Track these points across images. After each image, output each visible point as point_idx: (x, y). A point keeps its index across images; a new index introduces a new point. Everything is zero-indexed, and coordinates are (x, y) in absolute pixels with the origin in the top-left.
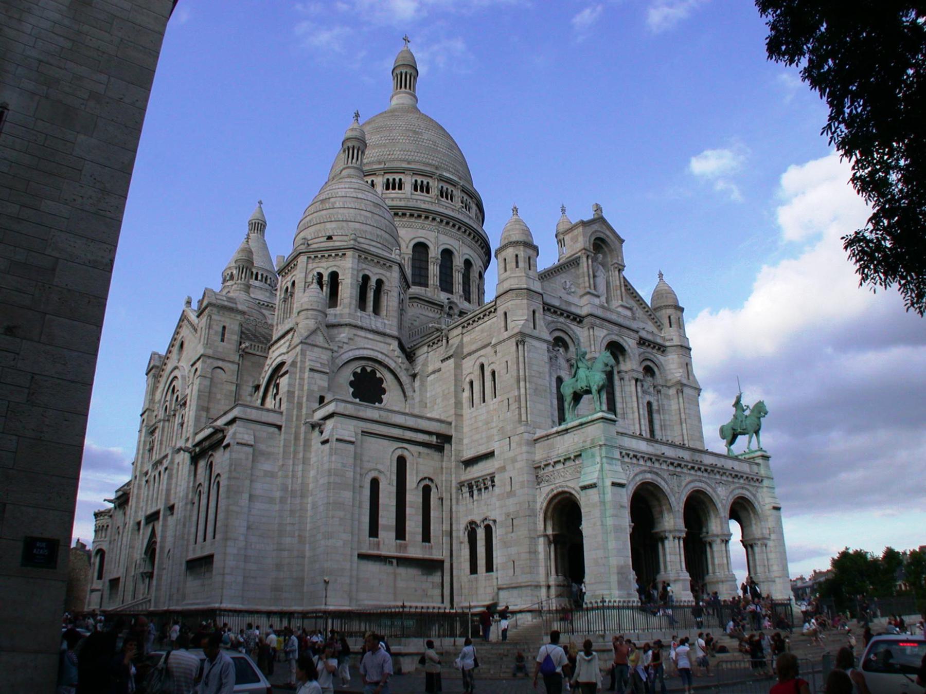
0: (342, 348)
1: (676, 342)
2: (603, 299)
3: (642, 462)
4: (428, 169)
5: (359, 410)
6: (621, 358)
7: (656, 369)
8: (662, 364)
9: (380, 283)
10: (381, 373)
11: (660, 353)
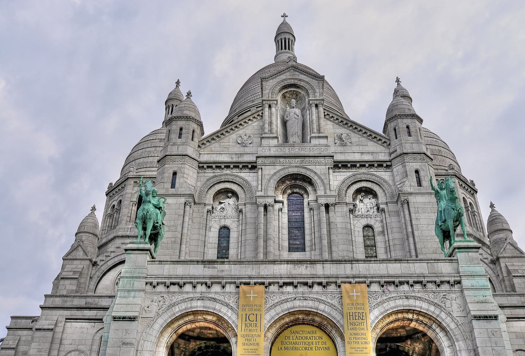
0: (109, 256)
1: (399, 152)
2: (295, 139)
5: (66, 302)
6: (309, 189)
8: (385, 181)
11: (381, 169)
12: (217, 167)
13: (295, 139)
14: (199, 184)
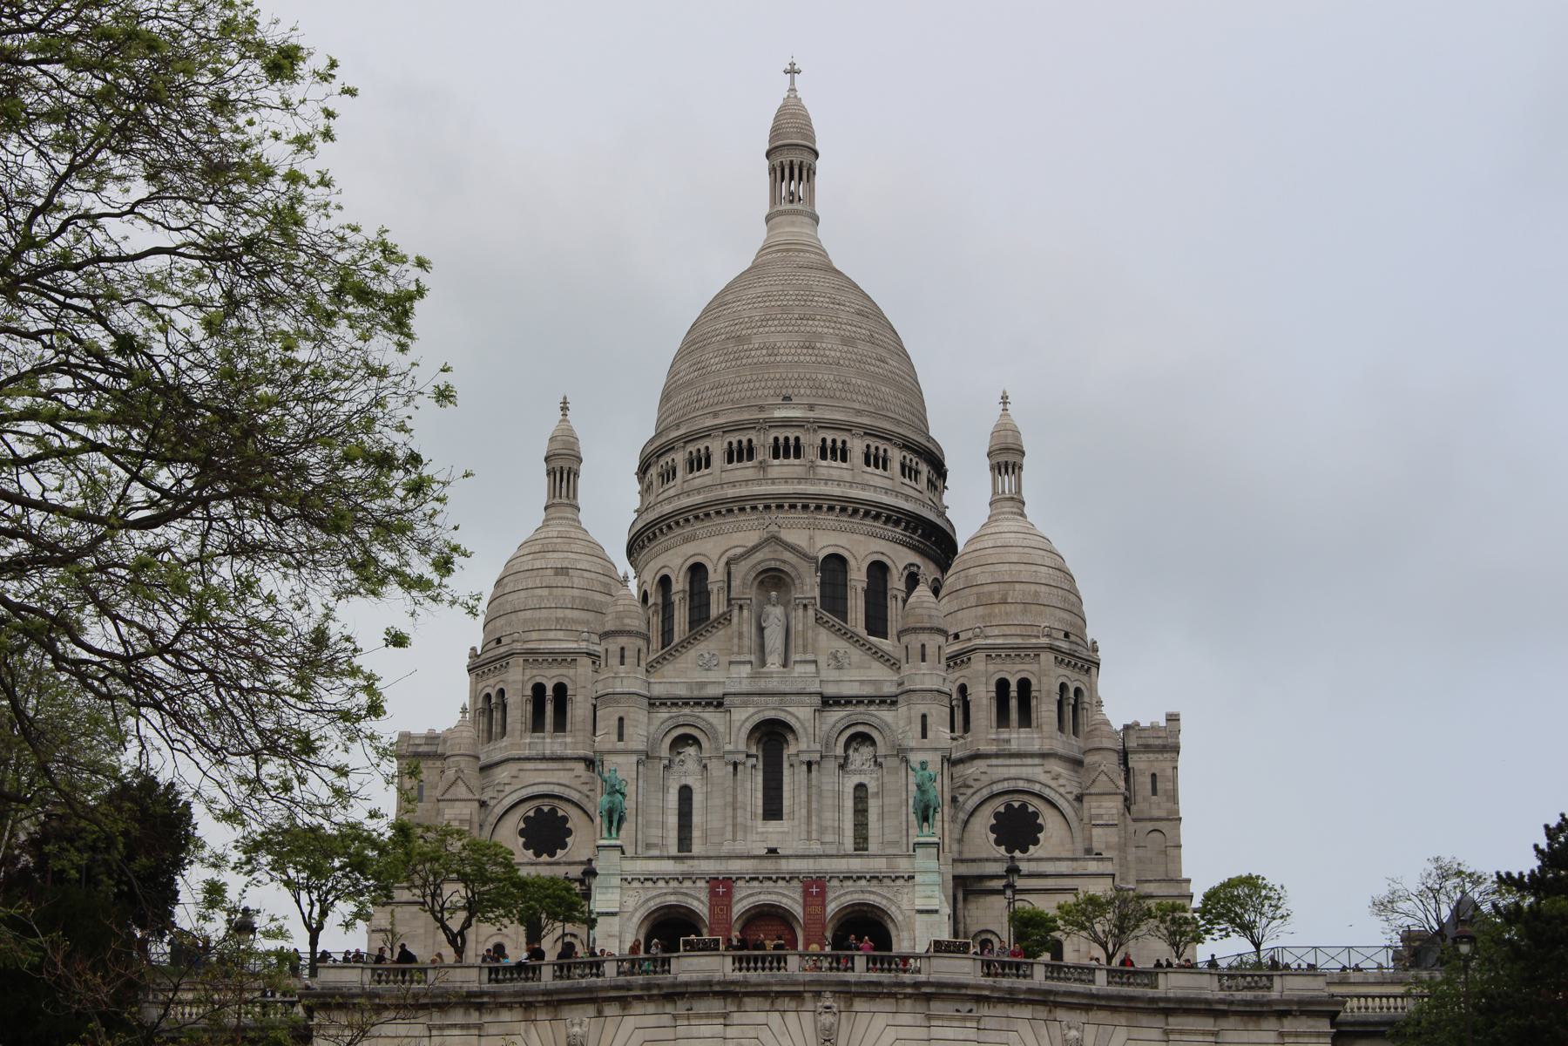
1: (907, 687)
3: (661, 884)
4: (746, 416)
6: (790, 737)
7: (875, 734)
8: (887, 725)
9: (560, 689)
10: (563, 810)
11: (885, 707)
12: (673, 704)
13: (774, 662)
14: (652, 729)
